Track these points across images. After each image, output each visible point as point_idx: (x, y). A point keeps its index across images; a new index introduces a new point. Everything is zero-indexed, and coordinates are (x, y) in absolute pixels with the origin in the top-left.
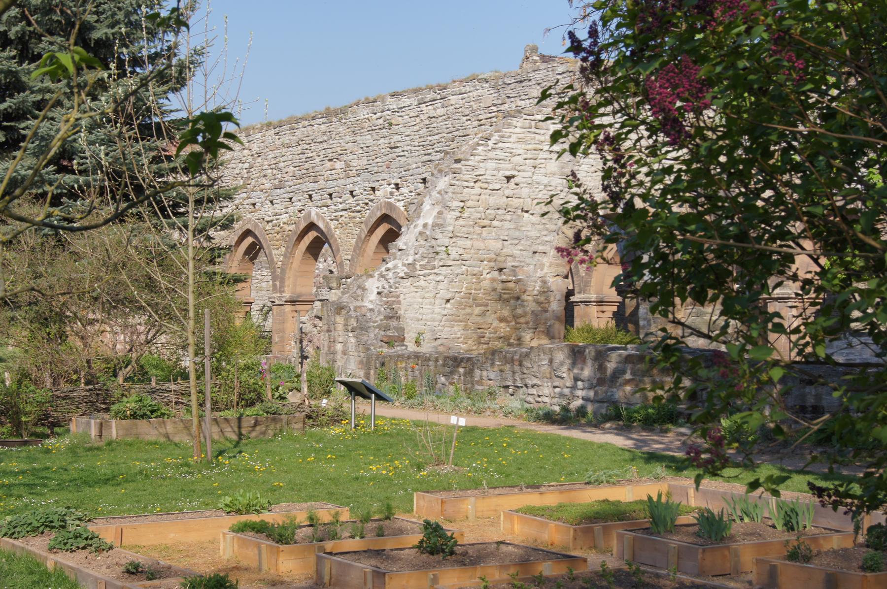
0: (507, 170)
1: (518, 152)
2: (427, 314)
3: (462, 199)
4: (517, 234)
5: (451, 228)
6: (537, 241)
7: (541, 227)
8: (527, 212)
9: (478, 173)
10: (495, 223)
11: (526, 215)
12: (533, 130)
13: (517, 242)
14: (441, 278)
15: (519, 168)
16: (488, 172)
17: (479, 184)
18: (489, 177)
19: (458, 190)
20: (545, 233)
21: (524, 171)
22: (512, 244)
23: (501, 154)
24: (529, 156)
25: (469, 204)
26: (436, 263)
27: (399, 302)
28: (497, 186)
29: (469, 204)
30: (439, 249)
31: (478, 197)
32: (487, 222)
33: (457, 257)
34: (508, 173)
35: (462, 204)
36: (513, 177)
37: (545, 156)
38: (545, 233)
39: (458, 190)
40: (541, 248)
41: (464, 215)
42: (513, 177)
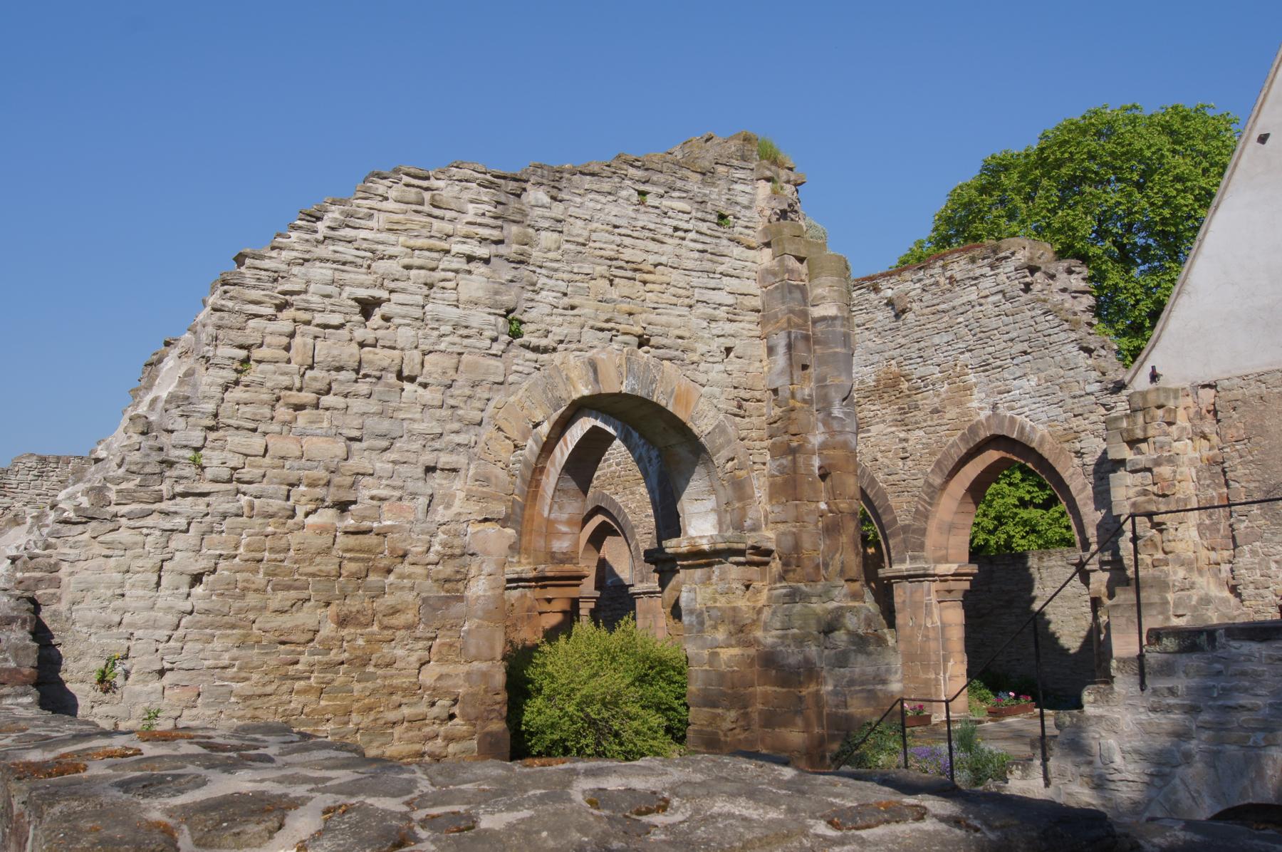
0: (361, 285)
1: (391, 250)
4: (385, 425)
6: (437, 445)
7: (445, 413)
8: (412, 379)
10: (327, 400)
12: (427, 208)
13: (385, 443)
14: (180, 522)
15: (392, 285)
17: (289, 313)
18: (316, 299)
19: (228, 319)
21: (403, 291)
22: (371, 449)
23: (348, 252)
26: (165, 488)
27: (57, 583)
28: (336, 319)
29: (257, 354)
30: (174, 454)
33: (225, 473)
34: (363, 293)
35: (242, 354)
36: (377, 302)
37: (455, 266)
38: (456, 426)
39: (228, 319)
40: (445, 459)
41: (245, 379)
42: (377, 302)
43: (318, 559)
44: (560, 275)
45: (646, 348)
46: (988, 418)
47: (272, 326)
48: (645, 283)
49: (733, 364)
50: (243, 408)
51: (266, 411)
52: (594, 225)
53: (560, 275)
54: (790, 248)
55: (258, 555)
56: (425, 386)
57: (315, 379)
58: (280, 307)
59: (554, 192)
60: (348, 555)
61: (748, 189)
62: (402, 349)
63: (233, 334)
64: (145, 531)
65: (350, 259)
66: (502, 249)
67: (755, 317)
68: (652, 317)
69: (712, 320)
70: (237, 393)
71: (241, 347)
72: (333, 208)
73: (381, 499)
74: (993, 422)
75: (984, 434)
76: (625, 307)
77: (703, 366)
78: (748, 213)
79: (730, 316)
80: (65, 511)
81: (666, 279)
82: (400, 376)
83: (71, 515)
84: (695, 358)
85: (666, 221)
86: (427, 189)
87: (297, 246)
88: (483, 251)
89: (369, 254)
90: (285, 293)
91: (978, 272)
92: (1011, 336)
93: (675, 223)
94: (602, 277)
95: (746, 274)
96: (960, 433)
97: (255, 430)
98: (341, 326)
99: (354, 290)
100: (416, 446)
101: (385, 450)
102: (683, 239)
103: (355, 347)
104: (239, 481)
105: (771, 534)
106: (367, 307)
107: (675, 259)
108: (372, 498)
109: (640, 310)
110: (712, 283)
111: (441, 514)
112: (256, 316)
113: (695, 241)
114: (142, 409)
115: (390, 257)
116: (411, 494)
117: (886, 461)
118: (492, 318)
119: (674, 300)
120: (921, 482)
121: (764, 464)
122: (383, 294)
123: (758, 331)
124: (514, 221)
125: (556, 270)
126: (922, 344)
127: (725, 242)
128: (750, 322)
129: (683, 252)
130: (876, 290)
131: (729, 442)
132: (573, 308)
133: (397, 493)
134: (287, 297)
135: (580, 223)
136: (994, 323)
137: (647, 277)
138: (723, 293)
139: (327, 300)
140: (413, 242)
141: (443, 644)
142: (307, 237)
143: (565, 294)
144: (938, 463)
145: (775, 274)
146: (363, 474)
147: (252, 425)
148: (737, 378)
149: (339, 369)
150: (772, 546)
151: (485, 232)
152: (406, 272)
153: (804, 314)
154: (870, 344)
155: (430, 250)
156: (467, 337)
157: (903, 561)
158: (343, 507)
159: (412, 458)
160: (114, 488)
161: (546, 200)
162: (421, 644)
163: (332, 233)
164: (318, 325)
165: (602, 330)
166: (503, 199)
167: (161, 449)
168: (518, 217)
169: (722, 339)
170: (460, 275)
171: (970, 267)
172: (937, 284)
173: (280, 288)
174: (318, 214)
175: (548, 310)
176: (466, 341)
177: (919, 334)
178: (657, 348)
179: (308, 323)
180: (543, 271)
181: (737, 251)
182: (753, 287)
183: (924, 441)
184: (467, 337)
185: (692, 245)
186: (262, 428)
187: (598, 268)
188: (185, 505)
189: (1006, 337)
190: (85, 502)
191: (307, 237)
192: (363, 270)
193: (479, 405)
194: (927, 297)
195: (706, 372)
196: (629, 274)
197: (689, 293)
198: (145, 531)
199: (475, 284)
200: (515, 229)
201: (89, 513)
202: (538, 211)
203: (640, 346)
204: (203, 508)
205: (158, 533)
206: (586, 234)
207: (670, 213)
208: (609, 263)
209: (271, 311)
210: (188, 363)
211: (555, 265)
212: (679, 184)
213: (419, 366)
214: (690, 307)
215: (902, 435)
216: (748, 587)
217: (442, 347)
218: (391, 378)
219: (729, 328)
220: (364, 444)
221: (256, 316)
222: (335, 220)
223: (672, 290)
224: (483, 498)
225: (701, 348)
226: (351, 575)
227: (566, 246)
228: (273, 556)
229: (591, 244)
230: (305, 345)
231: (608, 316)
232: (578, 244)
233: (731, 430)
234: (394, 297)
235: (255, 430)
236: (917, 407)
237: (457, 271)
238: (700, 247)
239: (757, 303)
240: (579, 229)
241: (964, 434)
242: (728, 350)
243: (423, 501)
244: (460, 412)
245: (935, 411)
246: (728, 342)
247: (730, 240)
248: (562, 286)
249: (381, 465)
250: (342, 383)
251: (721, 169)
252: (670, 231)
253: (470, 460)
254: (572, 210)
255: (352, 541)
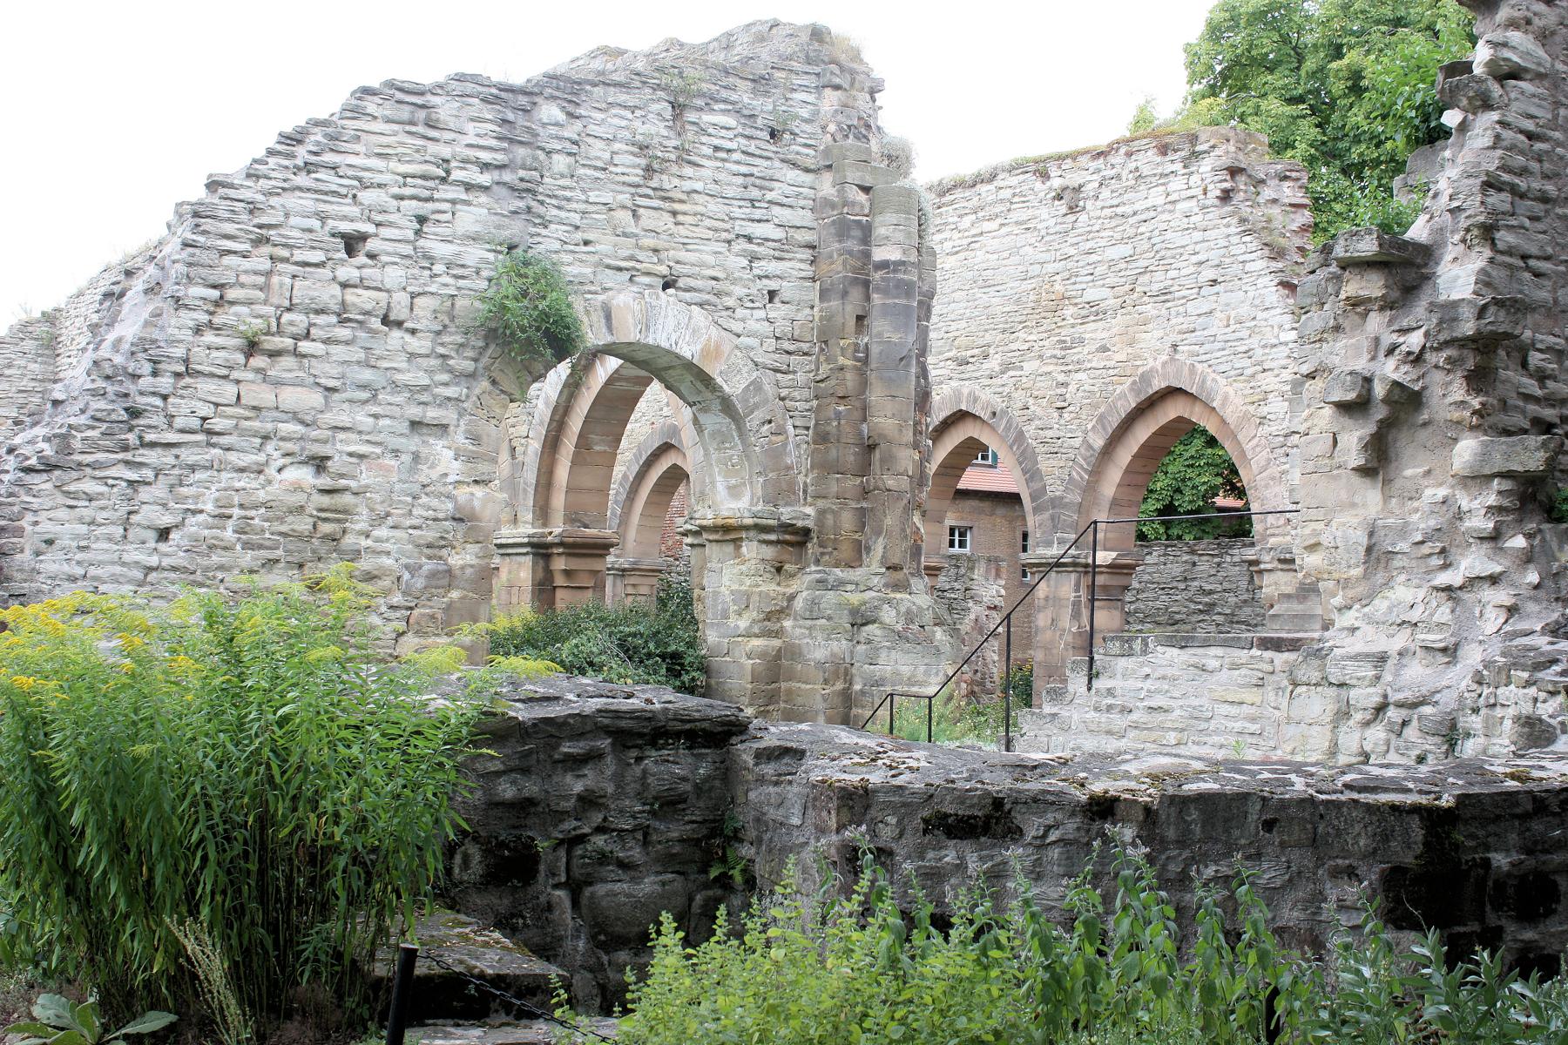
0: (345, 218)
1: (379, 178)
2: (100, 564)
3: (213, 279)
4: (366, 375)
5: (179, 352)
6: (425, 397)
7: (434, 362)
8: (399, 324)
9: (264, 220)
10: (304, 346)
11: (396, 334)
12: (421, 129)
13: (365, 395)
14: (148, 474)
15: (379, 218)
16: (293, 221)
17: (266, 250)
19: (204, 257)
20: (445, 377)
21: (390, 224)
22: (350, 401)
24: (408, 191)
25: (231, 294)
26: (132, 438)
27: (19, 532)
28: (318, 256)
30: (142, 401)
31: (261, 280)
32: (289, 342)
33: (195, 423)
34: (346, 227)
35: (215, 293)
36: (364, 237)
37: (450, 196)
39: (204, 257)
40: (432, 414)
42: (364, 237)
43: (290, 519)
44: (574, 205)
45: (671, 291)
46: (1164, 364)
47: (246, 264)
48: (674, 213)
49: (777, 311)
50: (215, 354)
51: (241, 358)
52: (617, 146)
53: (574, 205)
54: (853, 176)
55: (227, 511)
56: (413, 332)
57: (291, 323)
58: (260, 241)
59: (571, 108)
60: (323, 515)
61: (811, 98)
62: (388, 291)
63: (203, 272)
64: (110, 482)
65: (334, 188)
66: (507, 177)
67: (807, 254)
68: (682, 255)
69: (754, 258)
70: (209, 338)
71: (214, 287)
72: (316, 130)
73: (362, 457)
74: (1171, 369)
75: (1158, 384)
76: (649, 241)
77: (740, 312)
78: (808, 128)
79: (777, 254)
80: (27, 458)
81: (700, 209)
82: (385, 321)
83: (33, 461)
84: (730, 302)
85: (704, 139)
86: (423, 107)
87: (273, 174)
88: (485, 179)
89: (356, 183)
90: (260, 227)
91: (1170, 168)
92: (1201, 257)
93: (717, 142)
94: (624, 207)
95: (802, 203)
96: (1131, 380)
97: (225, 377)
98: (321, 265)
99: (336, 223)
100: (399, 399)
101: (366, 402)
102: (724, 160)
103: (337, 290)
104: (210, 432)
105: (809, 510)
106: (352, 243)
107: (713, 186)
108: (351, 455)
109: (666, 245)
110: (758, 214)
111: (425, 474)
112: (230, 252)
113: (738, 163)
114: (105, 351)
115: (380, 186)
116: (393, 451)
117: (1039, 412)
118: (491, 256)
119: (710, 234)
120: (1077, 442)
121: (808, 428)
122: (369, 228)
123: (808, 271)
124: (521, 143)
125: (568, 200)
126: (1093, 258)
127: (777, 164)
128: (802, 261)
129: (722, 176)
130: (1044, 176)
131: (766, 401)
132: (586, 243)
133: (378, 450)
134: (263, 232)
135: (600, 144)
136: (1177, 239)
137: (677, 206)
138: (770, 226)
139: (308, 236)
140: (404, 168)
141: (423, 615)
142: (286, 163)
143: (577, 228)
144: (1101, 418)
145: (833, 206)
146: (343, 429)
147: (224, 372)
148: (783, 327)
149: (319, 312)
150: (810, 524)
151: (485, 156)
152: (395, 203)
153: (867, 255)
154: (1029, 250)
155: (424, 177)
156: (463, 277)
157: (1049, 544)
158: (319, 463)
159: (396, 411)
160: (79, 435)
161: (561, 117)
162: (398, 614)
163: (313, 159)
164: (297, 263)
165: (620, 269)
166: (510, 116)
167: (126, 395)
168: (526, 138)
169: (765, 281)
170: (458, 207)
171: (1159, 159)
172: (1118, 177)
173: (256, 221)
174: (299, 137)
175: (557, 245)
176: (461, 283)
177: (1089, 245)
178: (686, 290)
179: (285, 260)
180: (554, 202)
181: (793, 175)
182: (805, 217)
183: (1087, 387)
184: (463, 277)
185: (735, 168)
186: (235, 375)
187: (620, 197)
188: (151, 456)
189: (1194, 259)
190: (49, 450)
191: (286, 163)
192: (348, 200)
193: (471, 354)
194: (1105, 193)
195: (743, 320)
196: (656, 203)
197: (727, 226)
198: (110, 482)
199: (473, 216)
200: (521, 152)
201: (53, 461)
202: (553, 130)
203: (666, 286)
204: (172, 461)
205: (124, 484)
206: (607, 156)
207: (711, 130)
208: (633, 190)
209: (247, 246)
210: (157, 303)
211: (568, 194)
212: (724, 94)
213: (407, 311)
214: (729, 242)
215: (1061, 378)
216: (779, 570)
217: (433, 289)
218: (375, 323)
219: (773, 267)
220: (344, 396)
221: (230, 252)
222: (318, 143)
223: (708, 222)
224: (471, 458)
225: (739, 291)
226: (325, 537)
227: (582, 171)
228: (243, 513)
229: (612, 169)
230: (281, 285)
231: (627, 253)
232: (596, 168)
233: (769, 389)
234: (385, 232)
235: (225, 377)
236: (1082, 341)
237: (453, 202)
238: (744, 169)
239: (808, 237)
240: (598, 151)
241: (1134, 383)
242: (772, 295)
243: (406, 458)
244: (451, 362)
245: (1104, 349)
246: (773, 285)
247: (783, 161)
248: (575, 218)
249: (362, 418)
250: (322, 327)
251: (778, 74)
252: (710, 151)
253: (460, 415)
254: (592, 129)
255: (326, 500)
